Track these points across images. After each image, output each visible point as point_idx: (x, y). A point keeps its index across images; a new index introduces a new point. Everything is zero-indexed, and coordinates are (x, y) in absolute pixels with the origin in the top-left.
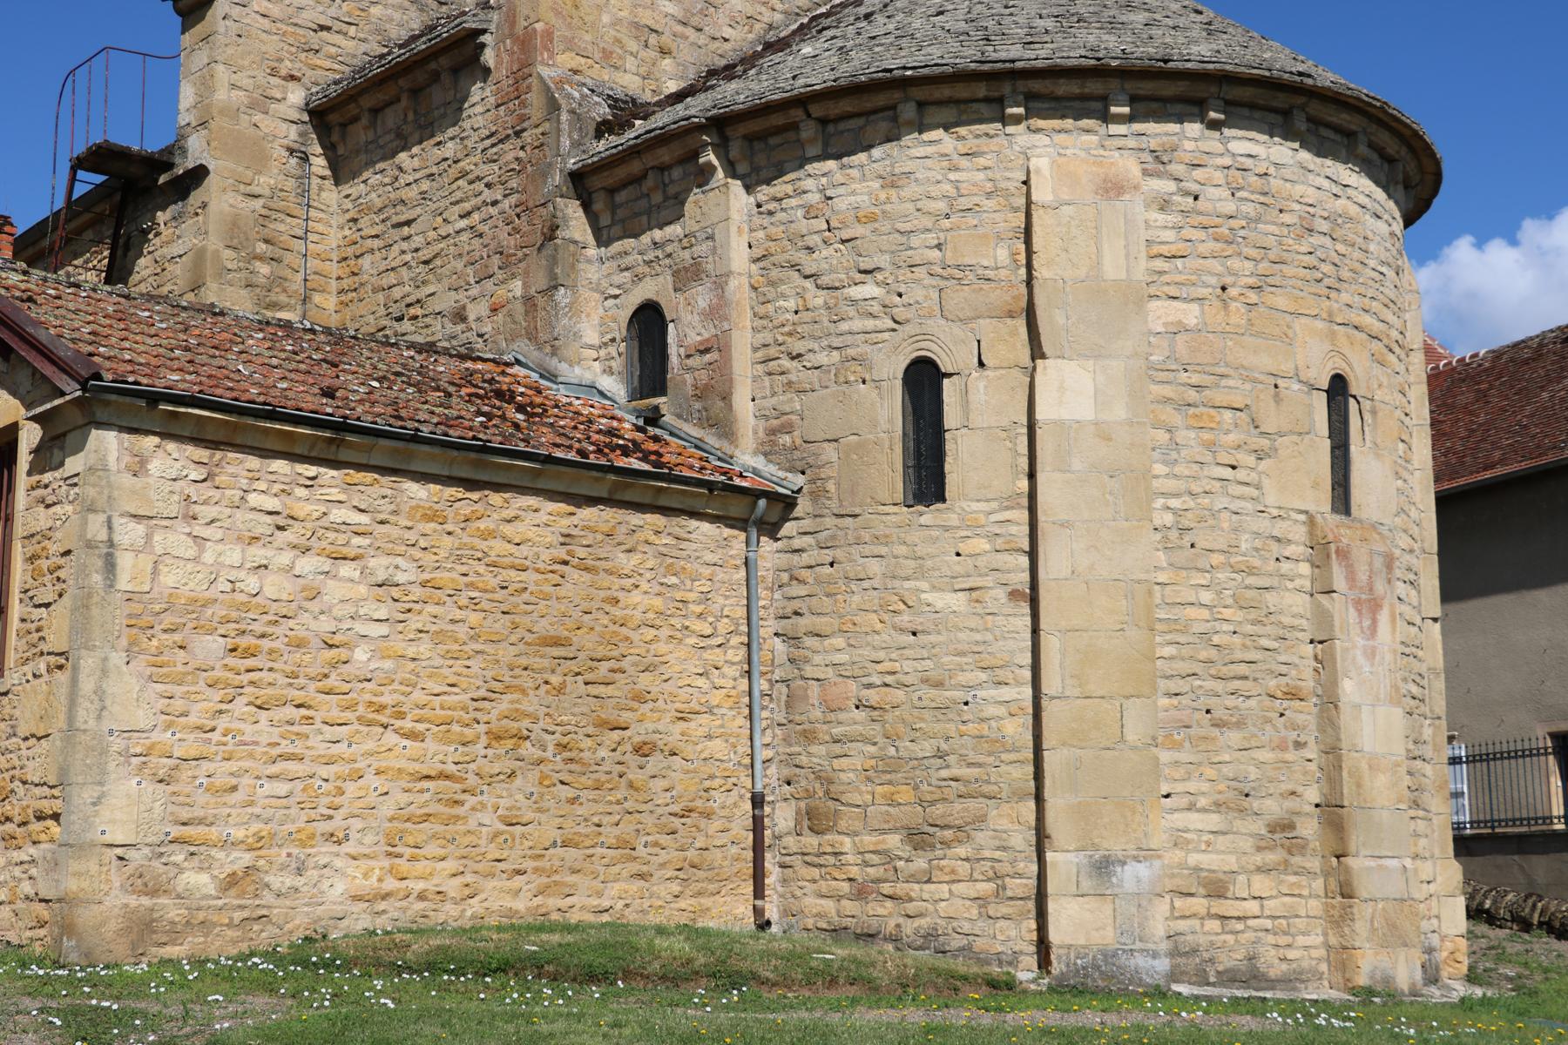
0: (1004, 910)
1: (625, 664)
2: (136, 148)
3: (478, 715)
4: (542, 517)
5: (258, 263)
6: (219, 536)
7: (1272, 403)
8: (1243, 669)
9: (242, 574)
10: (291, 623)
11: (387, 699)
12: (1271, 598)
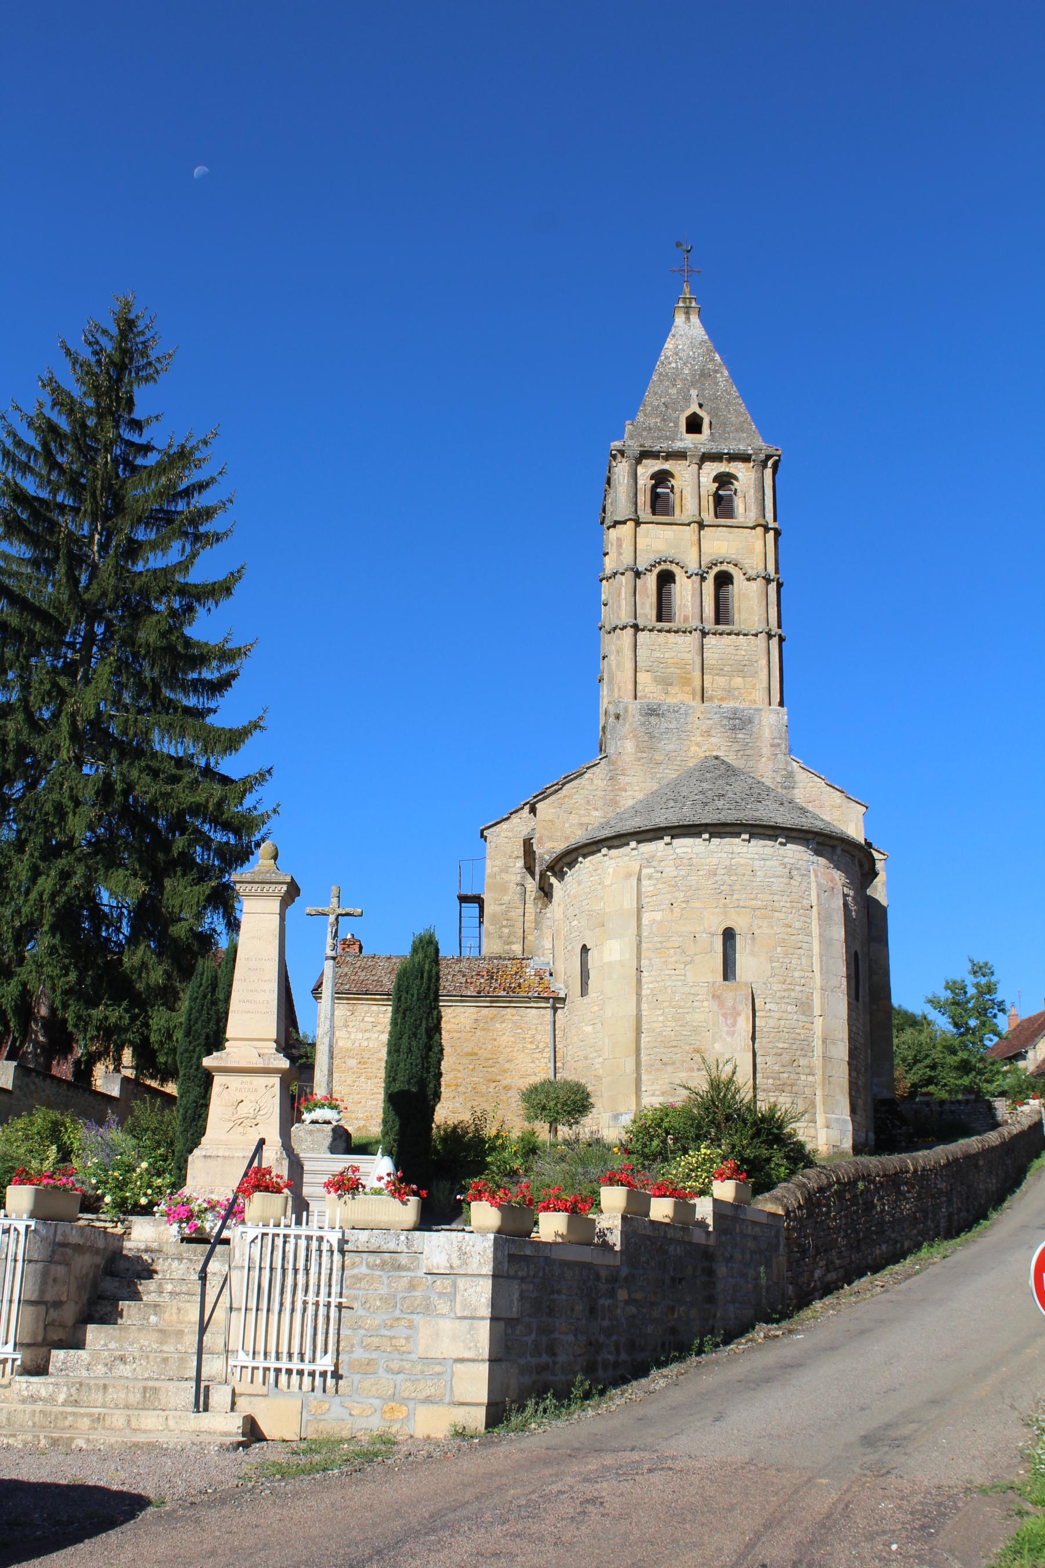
2: (469, 894)
4: (467, 1015)
8: (675, 1043)
12: (688, 1017)
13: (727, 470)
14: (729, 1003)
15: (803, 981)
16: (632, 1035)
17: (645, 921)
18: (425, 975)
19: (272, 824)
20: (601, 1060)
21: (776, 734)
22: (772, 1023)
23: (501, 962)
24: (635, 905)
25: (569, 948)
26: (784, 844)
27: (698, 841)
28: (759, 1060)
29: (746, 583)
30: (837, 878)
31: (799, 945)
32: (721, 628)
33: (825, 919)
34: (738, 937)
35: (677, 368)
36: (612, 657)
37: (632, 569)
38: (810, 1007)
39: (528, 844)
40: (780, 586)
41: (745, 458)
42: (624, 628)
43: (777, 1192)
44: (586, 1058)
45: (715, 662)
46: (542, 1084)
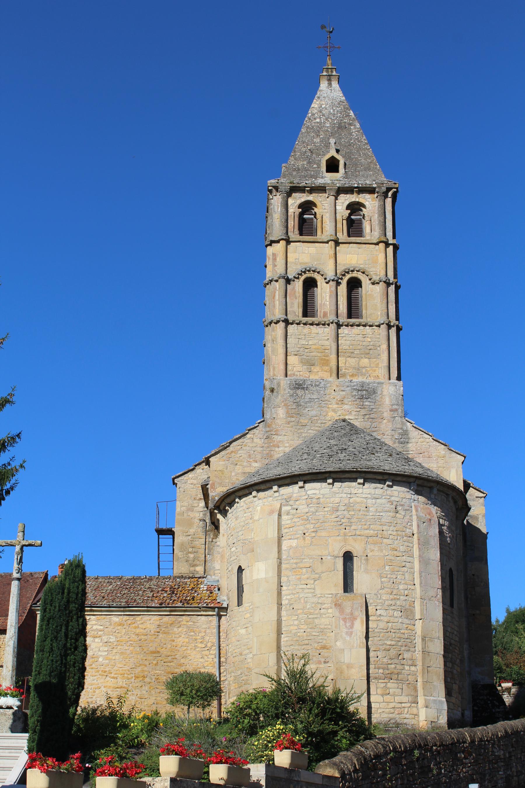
1: (176, 657)
2: (164, 528)
3: (132, 672)
4: (151, 621)
5: (190, 554)
7: (320, 564)
11: (107, 669)
12: (316, 621)
13: (357, 200)
14: (348, 610)
15: (406, 592)
16: (274, 636)
17: (284, 547)
18: (66, 591)
19: (20, 476)
20: (251, 656)
21: (394, 402)
22: (382, 625)
23: (182, 580)
24: (276, 535)
25: (230, 569)
26: (391, 487)
27: (324, 485)
28: (372, 654)
29: (371, 286)
30: (434, 512)
31: (404, 564)
32: (352, 321)
33: (423, 544)
34: (355, 558)
35: (320, 123)
36: (269, 345)
37: (283, 277)
38: (413, 613)
39: (205, 489)
40: (397, 288)
41: (371, 191)
42: (277, 322)
43: (336, 759)
44: (241, 654)
45: (347, 347)
46: (182, 675)
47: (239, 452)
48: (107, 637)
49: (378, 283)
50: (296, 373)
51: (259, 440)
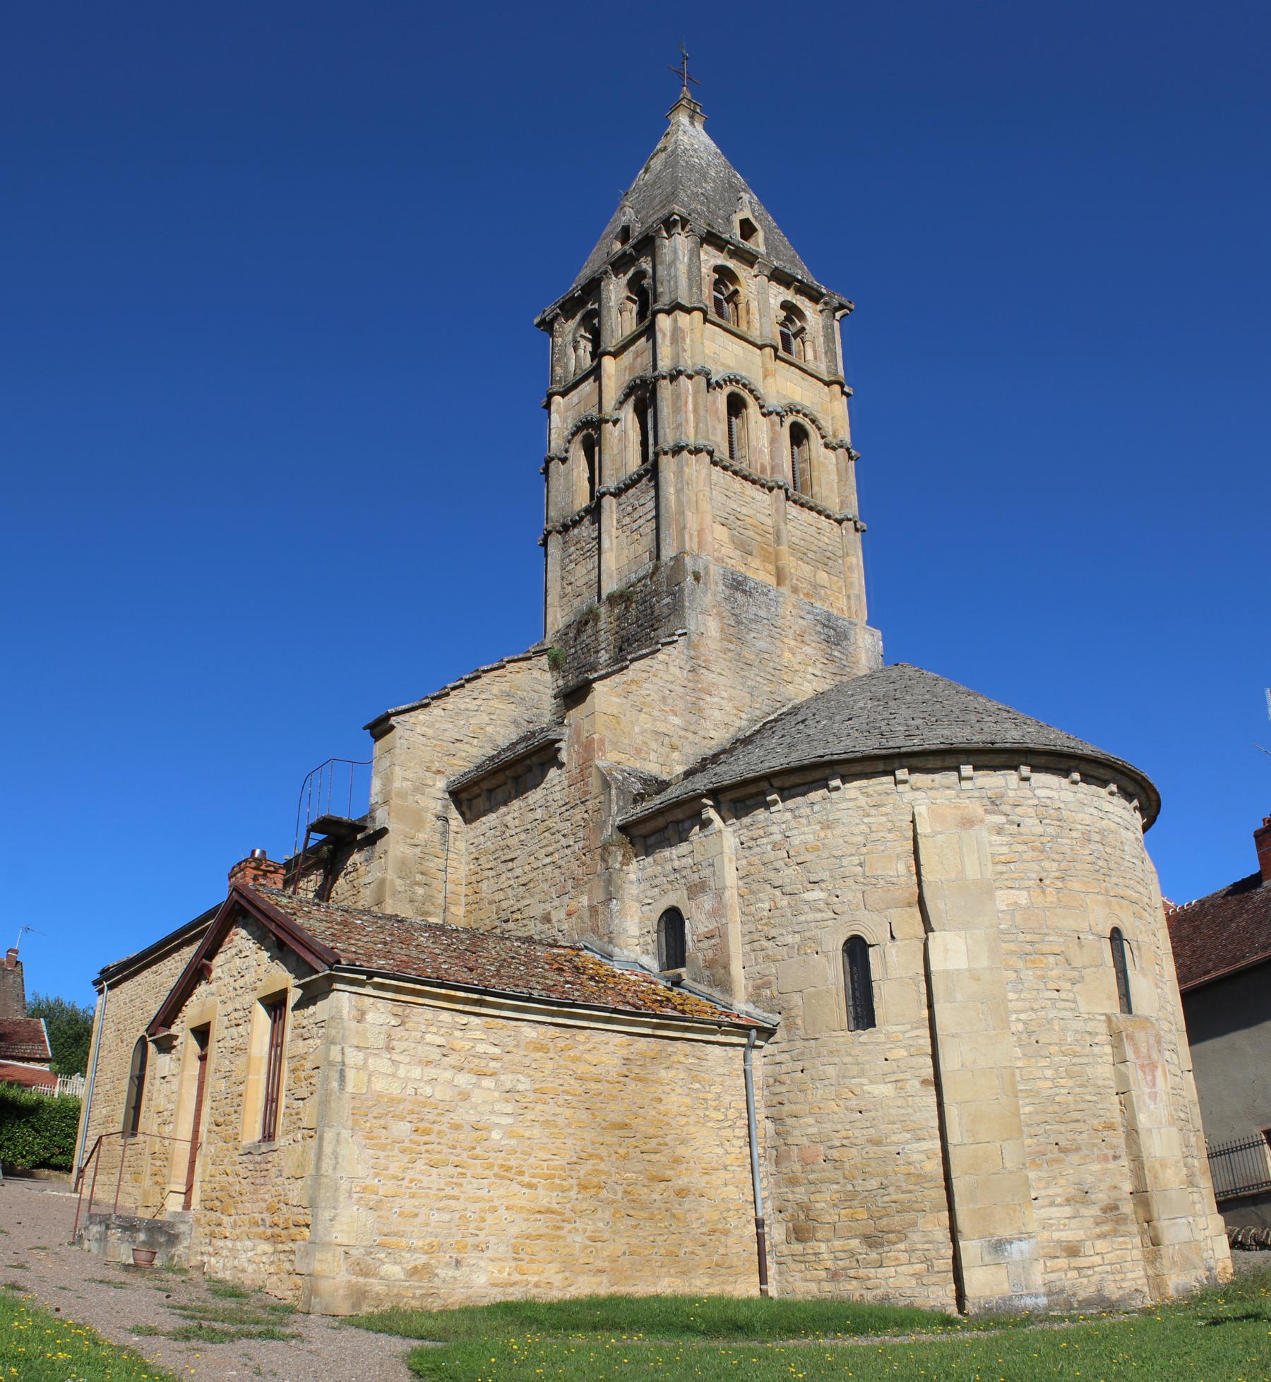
0: (934, 1279)
1: (667, 1140)
3: (573, 1173)
6: (407, 1060)
9: (422, 1084)
10: (452, 1115)
29: (823, 449)
45: (797, 541)
47: (646, 685)
48: (510, 1077)
49: (834, 449)
50: (726, 559)
51: (677, 671)
